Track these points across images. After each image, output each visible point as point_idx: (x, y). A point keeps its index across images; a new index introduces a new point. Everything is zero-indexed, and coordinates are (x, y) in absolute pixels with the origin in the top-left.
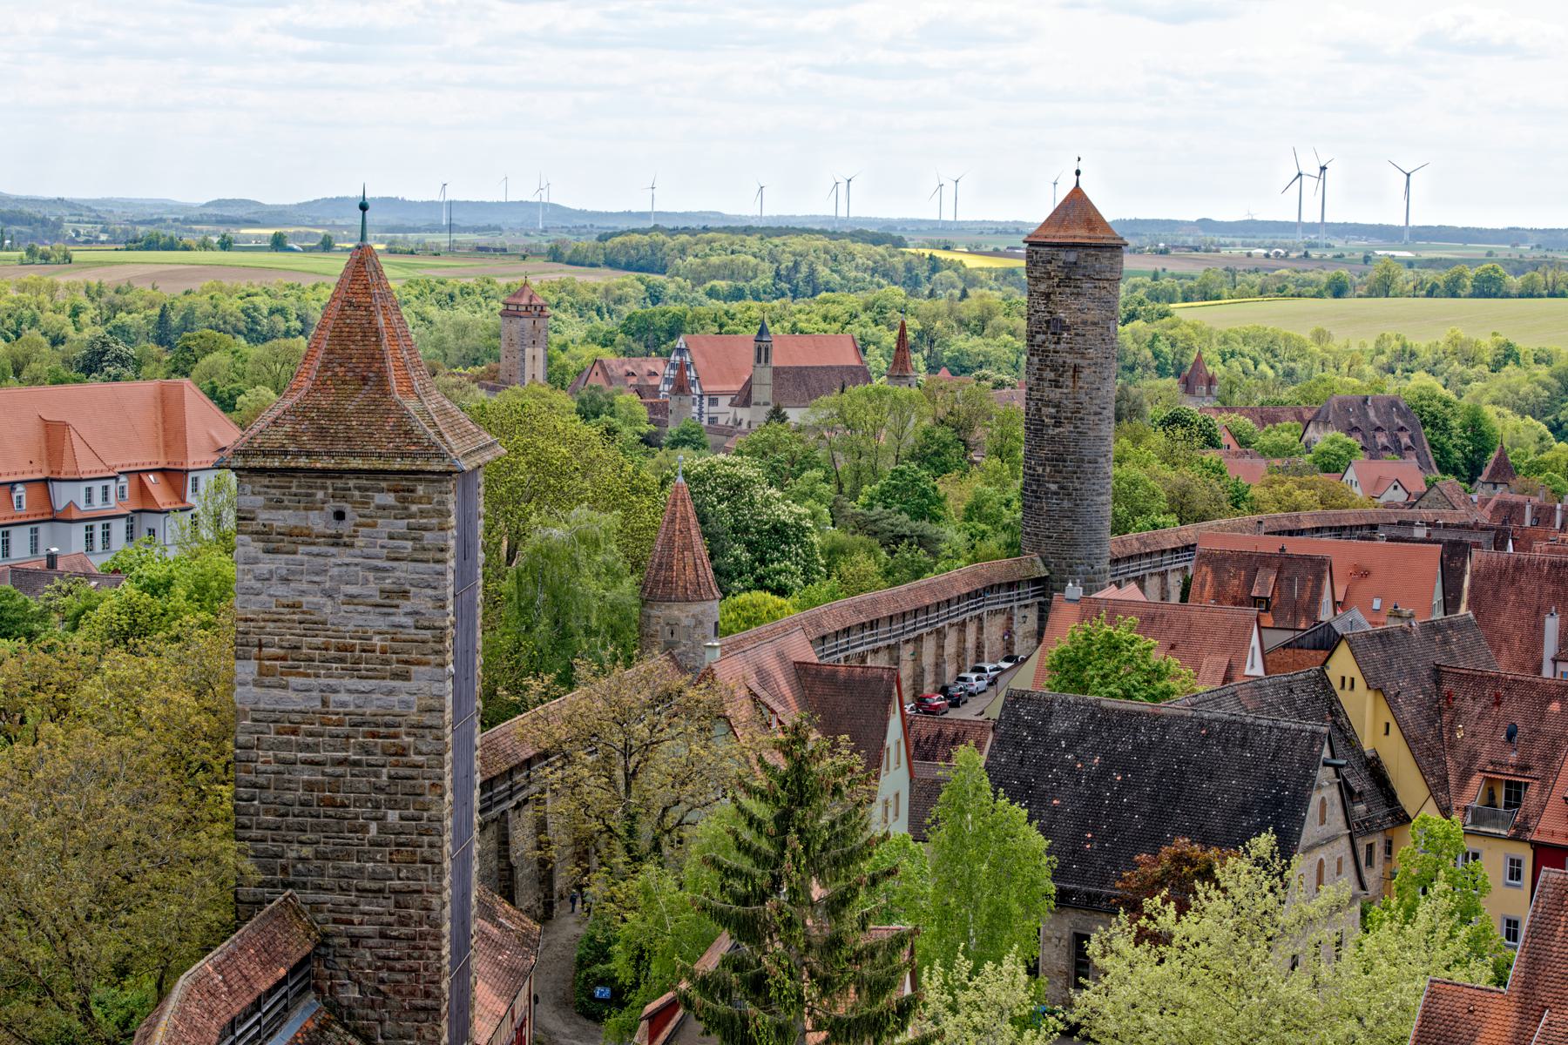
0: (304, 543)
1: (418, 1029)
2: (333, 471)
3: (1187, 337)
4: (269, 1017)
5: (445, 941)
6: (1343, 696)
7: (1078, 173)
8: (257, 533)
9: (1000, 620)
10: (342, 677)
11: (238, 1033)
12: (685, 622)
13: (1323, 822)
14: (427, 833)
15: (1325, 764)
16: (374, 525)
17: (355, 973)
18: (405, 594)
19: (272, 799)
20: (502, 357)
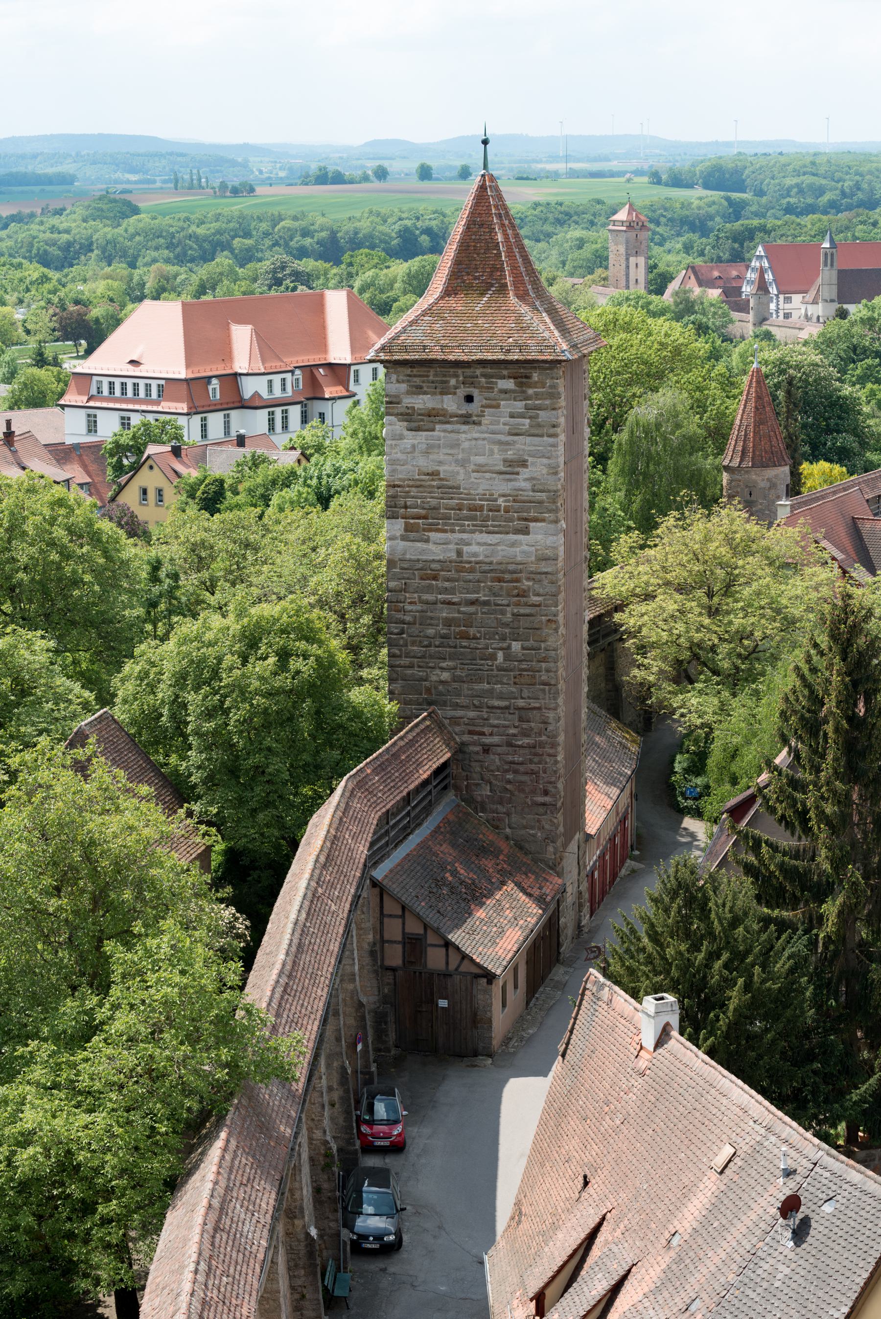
1: (539, 821)
2: (463, 362)
4: (417, 810)
5: (560, 749)
8: (402, 414)
10: (473, 532)
11: (391, 823)
12: (762, 484)
14: (544, 660)
16: (498, 406)
17: (487, 775)
18: (524, 464)
19: (417, 633)
20: (610, 266)
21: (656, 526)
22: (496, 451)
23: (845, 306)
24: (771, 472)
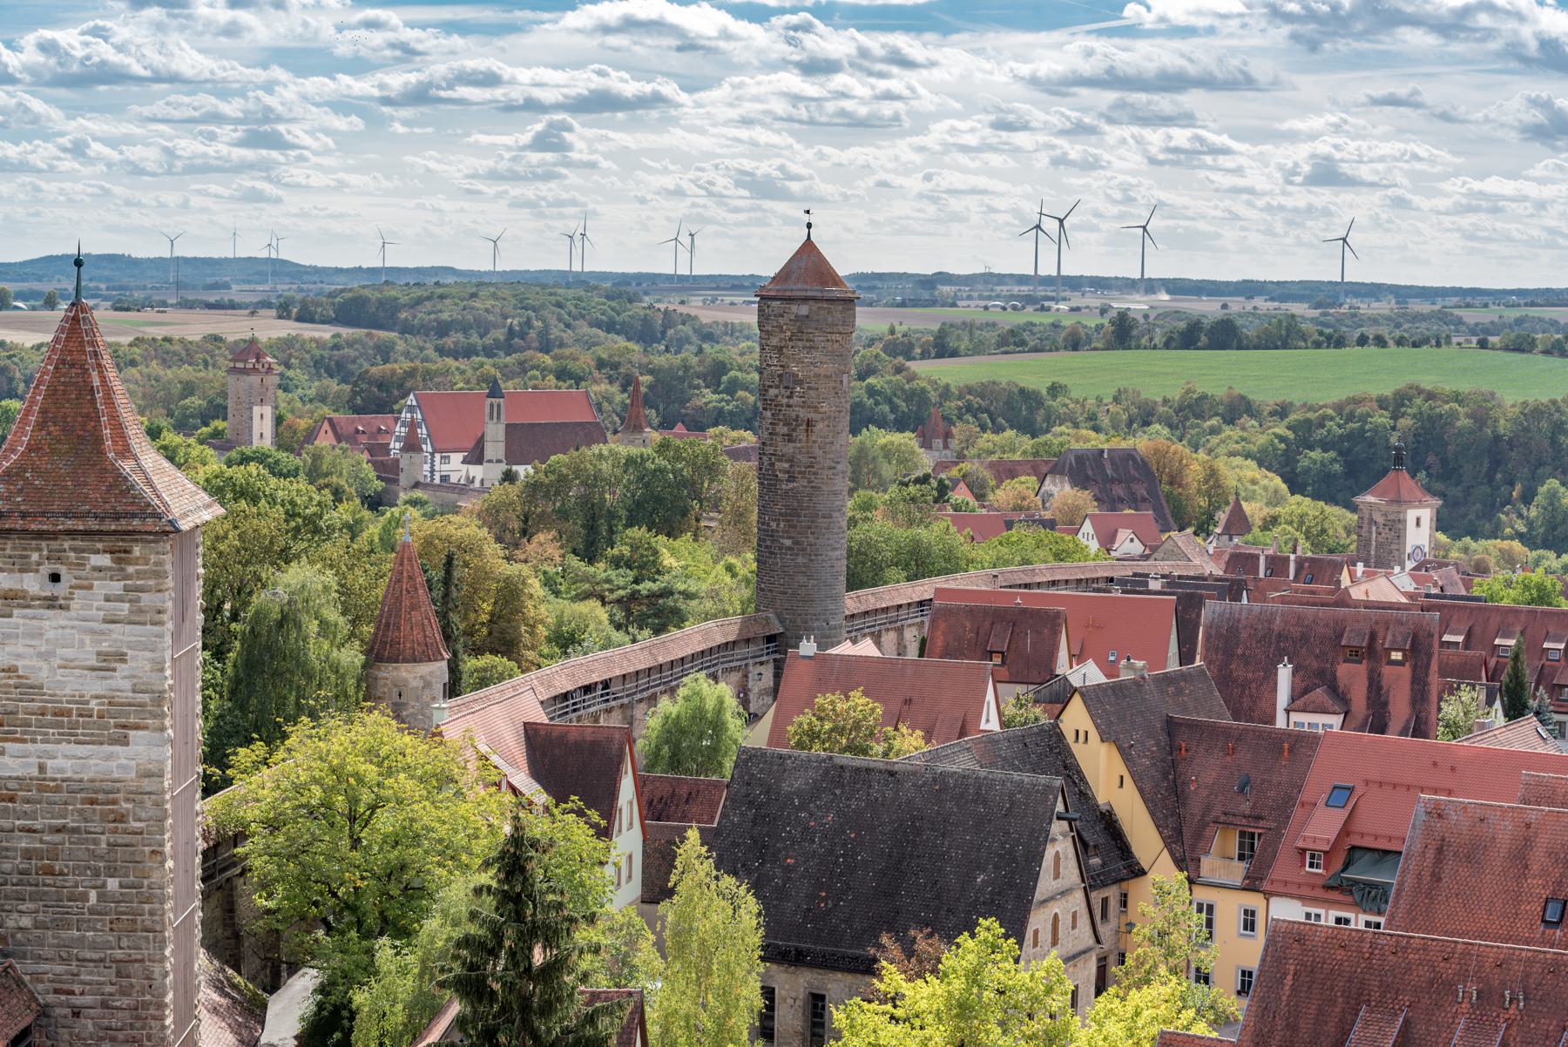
0: (19, 606)
3: (923, 390)
6: (1077, 749)
7: (809, 226)
9: (736, 677)
10: (58, 742)
13: (1057, 876)
15: (1059, 818)
16: (90, 587)
18: (121, 657)
21: (285, 736)
22: (88, 642)
23: (515, 468)
24: (424, 669)
